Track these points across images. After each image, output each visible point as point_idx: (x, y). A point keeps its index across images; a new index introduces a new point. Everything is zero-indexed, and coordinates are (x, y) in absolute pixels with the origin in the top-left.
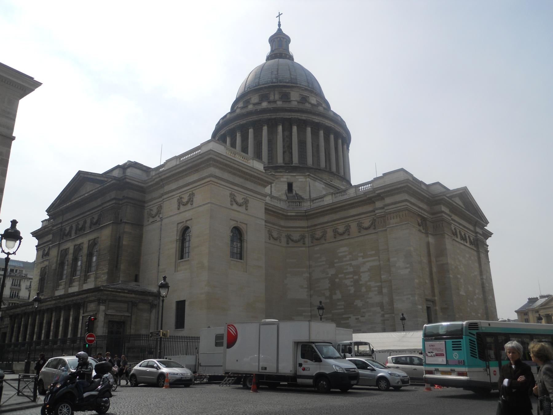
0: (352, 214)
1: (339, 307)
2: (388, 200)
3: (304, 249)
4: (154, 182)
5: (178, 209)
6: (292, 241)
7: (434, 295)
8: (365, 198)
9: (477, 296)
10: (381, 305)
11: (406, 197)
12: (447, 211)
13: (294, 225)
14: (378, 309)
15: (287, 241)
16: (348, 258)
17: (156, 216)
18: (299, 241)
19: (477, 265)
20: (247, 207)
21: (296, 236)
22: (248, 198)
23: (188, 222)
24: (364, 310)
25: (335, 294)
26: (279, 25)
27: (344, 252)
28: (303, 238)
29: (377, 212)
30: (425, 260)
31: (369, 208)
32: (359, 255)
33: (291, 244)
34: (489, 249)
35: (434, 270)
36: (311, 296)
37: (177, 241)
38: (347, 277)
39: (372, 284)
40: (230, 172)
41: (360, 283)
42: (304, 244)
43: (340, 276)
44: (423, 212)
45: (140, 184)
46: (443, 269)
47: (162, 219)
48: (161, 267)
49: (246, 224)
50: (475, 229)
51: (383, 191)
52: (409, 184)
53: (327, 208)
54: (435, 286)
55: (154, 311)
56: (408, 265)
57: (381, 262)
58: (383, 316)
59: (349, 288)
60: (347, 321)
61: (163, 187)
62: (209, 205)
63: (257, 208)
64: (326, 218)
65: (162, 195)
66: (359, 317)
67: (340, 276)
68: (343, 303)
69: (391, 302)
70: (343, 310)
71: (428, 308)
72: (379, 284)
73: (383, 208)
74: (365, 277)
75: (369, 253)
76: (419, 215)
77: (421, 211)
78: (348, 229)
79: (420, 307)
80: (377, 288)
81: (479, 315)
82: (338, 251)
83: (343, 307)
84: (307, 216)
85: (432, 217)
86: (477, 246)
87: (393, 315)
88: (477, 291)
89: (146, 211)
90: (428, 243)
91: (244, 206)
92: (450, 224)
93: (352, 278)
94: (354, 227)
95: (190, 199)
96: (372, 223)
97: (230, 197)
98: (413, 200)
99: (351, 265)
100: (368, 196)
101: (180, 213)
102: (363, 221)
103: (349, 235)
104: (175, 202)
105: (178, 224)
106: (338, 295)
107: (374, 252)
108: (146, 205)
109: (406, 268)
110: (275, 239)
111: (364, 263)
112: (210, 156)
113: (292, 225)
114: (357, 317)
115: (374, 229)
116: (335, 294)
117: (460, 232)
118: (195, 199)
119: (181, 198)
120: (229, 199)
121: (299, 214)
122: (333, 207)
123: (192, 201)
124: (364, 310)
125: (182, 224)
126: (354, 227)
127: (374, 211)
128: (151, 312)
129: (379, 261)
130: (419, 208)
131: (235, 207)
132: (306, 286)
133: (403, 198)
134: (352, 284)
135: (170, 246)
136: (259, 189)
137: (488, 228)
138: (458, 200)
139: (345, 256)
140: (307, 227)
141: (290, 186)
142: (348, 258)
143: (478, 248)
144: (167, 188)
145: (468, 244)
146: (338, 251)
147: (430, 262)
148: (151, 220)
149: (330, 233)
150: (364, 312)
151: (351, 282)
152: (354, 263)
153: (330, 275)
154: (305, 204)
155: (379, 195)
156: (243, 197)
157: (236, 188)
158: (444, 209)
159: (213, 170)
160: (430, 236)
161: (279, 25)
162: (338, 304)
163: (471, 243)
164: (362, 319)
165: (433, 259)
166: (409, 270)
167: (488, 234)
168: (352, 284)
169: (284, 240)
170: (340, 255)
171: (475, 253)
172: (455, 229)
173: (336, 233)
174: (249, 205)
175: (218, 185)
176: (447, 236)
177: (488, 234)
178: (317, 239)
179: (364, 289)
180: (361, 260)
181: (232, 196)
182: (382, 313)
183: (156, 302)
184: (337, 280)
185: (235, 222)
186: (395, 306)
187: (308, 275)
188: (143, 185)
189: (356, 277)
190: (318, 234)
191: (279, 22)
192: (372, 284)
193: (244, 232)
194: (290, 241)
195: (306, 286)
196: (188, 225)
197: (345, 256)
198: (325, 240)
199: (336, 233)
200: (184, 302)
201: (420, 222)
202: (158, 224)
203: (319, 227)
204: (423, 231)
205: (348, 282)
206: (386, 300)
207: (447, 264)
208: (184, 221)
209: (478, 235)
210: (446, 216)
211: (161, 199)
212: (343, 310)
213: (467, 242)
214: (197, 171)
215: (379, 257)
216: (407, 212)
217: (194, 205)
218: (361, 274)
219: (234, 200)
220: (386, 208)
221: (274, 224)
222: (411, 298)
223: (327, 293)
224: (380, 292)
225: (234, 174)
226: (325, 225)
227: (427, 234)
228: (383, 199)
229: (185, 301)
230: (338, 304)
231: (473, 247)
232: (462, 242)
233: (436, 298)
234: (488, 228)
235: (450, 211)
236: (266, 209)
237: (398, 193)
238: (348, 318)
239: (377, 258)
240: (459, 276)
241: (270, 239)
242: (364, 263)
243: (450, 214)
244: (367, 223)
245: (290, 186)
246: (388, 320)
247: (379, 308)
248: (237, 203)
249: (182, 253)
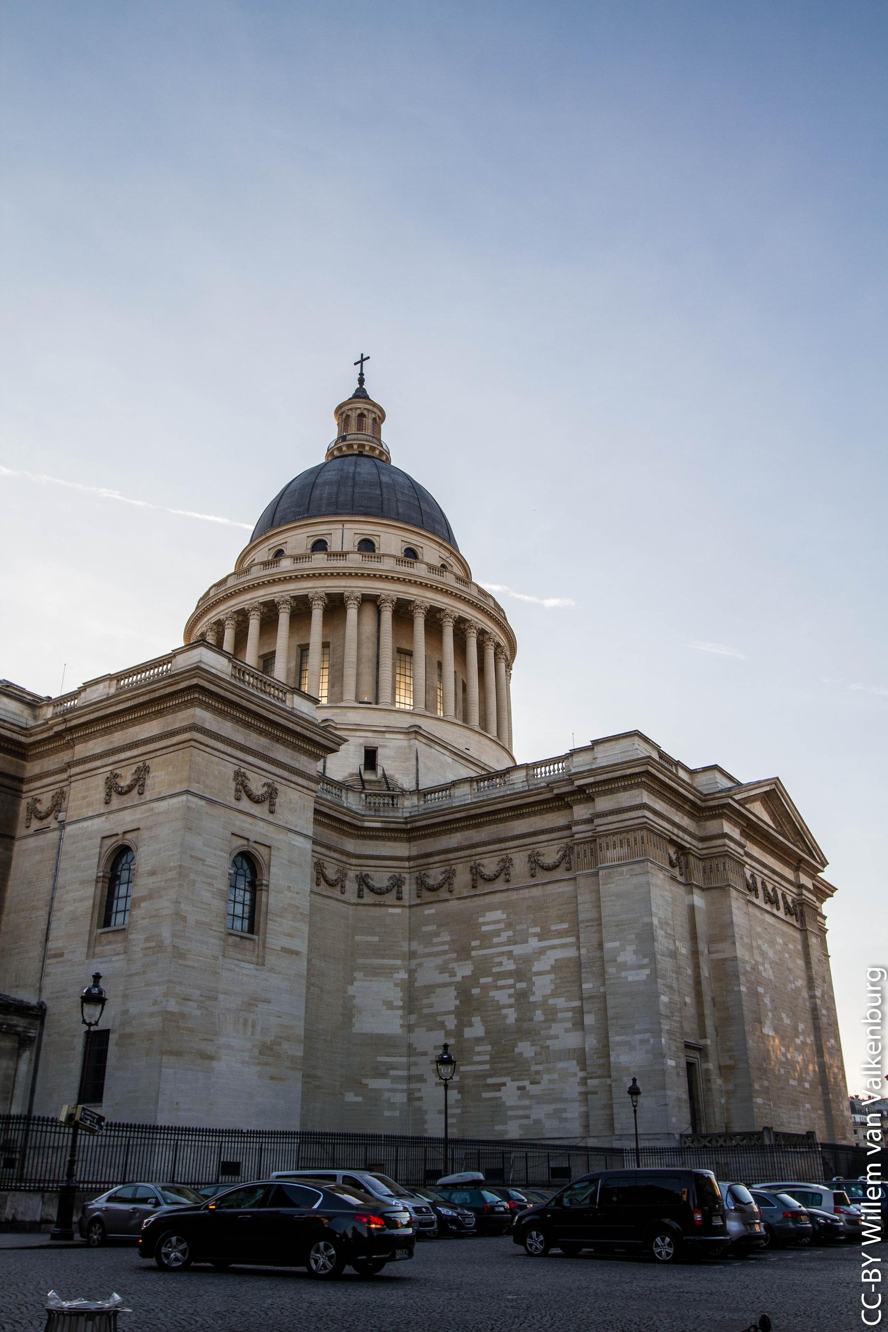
0: (516, 832)
1: (477, 1058)
2: (603, 804)
3: (398, 910)
4: (51, 733)
5: (107, 803)
6: (372, 890)
7: (704, 1036)
8: (549, 795)
9: (801, 1038)
10: (581, 1057)
11: (646, 797)
12: (736, 833)
13: (377, 853)
14: (572, 1066)
15: (360, 890)
16: (504, 937)
17: (47, 815)
18: (388, 890)
19: (800, 962)
20: (272, 804)
21: (380, 879)
22: (277, 785)
23: (128, 836)
24: (539, 1068)
25: (471, 1025)
26: (361, 381)
27: (494, 922)
28: (397, 883)
29: (575, 829)
30: (684, 950)
31: (557, 819)
32: (531, 930)
33: (369, 897)
34: (828, 924)
35: (705, 972)
36: (410, 1028)
37: (97, 882)
38: (500, 983)
39: (560, 1002)
40: (238, 721)
41: (532, 999)
42: (399, 898)
43: (483, 980)
44: (681, 834)
45: (15, 736)
46: (727, 971)
47: (62, 825)
48: (51, 945)
49: (269, 847)
50: (797, 877)
51: (591, 780)
52: (650, 769)
53: (458, 815)
54: (707, 1012)
55: (26, 1055)
56: (646, 961)
57: (583, 951)
58: (584, 1081)
59: (504, 1011)
60: (498, 1094)
61: (70, 745)
62: (184, 798)
63: (297, 807)
64: (455, 839)
65: (69, 765)
66: (526, 1083)
67: (483, 980)
68: (489, 1048)
69: (605, 1049)
70: (487, 1067)
71: (690, 1066)
72: (576, 1003)
73: (590, 821)
74: (543, 986)
75: (553, 928)
76: (672, 842)
77: (676, 831)
78: (505, 866)
79: (671, 1063)
80: (570, 1014)
81: (807, 1085)
82: (481, 920)
83: (487, 1058)
84: (410, 831)
85: (700, 845)
86: (801, 918)
87: (608, 1081)
88: (801, 1027)
89: (24, 803)
90: (692, 908)
91: (267, 803)
92: (742, 864)
93: (510, 987)
94: (520, 862)
95: (137, 780)
96: (564, 856)
97: (235, 779)
98: (660, 805)
99: (510, 954)
100: (556, 791)
101: (110, 813)
102: (542, 850)
103: (508, 881)
104: (97, 786)
105: (103, 838)
106: (476, 1029)
107: (565, 926)
108: (25, 788)
109: (641, 967)
110: (331, 884)
111: (542, 951)
112: (195, 681)
113: (371, 853)
114: (521, 1083)
115: (568, 870)
116: (471, 1025)
117: (763, 883)
118: (149, 782)
119: (116, 776)
120: (232, 785)
121: (393, 826)
122: (473, 812)
123: (143, 785)
124: (539, 1068)
125: (114, 839)
126: (520, 862)
127: (568, 827)
128: (19, 1056)
129: (578, 948)
130: (674, 824)
131: (245, 804)
132: (401, 1004)
133: (637, 801)
134: (512, 1001)
135: (79, 895)
136: (303, 762)
137: (826, 875)
138: (758, 810)
139: (497, 933)
140: (409, 859)
142: (504, 937)
143: (803, 923)
144: (82, 750)
145: (781, 914)
146: (481, 920)
147: (695, 953)
148: (36, 824)
149: (463, 876)
150: (537, 1073)
151: (510, 996)
152: (518, 950)
153: (458, 978)
154: (407, 803)
155: (581, 789)
156: (265, 780)
157: (250, 759)
158: (728, 828)
159: (201, 715)
160: (695, 890)
161: (361, 381)
162: (477, 1049)
164: (533, 1089)
165: (702, 947)
166: (647, 971)
167: (825, 891)
168: (512, 1001)
169: (351, 886)
170: (484, 928)
171: (797, 935)
172: (752, 876)
173: (478, 877)
174: (277, 800)
175: (208, 750)
176: (734, 893)
177: (825, 891)
178: (432, 889)
179: (539, 1016)
180: (534, 943)
181: (240, 778)
182: (581, 1074)
183: (33, 1033)
184: (475, 991)
185: (245, 842)
186: (612, 1059)
187: (406, 976)
188: (23, 739)
189: (522, 985)
190: (435, 875)
191: (361, 374)
192: (560, 1002)
193: (263, 866)
194: (366, 890)
195: (401, 1004)
196: (126, 842)
197: (497, 933)
198: (451, 891)
199: (478, 877)
200: (104, 1035)
201: (674, 857)
202: (53, 836)
203: (437, 858)
204: (679, 878)
205: (502, 997)
206: (591, 1042)
207: (735, 958)
208: (120, 832)
209: (805, 892)
210: (732, 845)
211: (64, 776)
212: (487, 1067)
213: (778, 909)
214: (160, 713)
215: (578, 938)
216: (645, 833)
217: (148, 796)
218: (534, 978)
219: (245, 787)
220: (597, 821)
221: (329, 848)
222: (651, 1040)
223: (451, 1023)
224: (579, 1024)
225: (248, 726)
226: (451, 856)
227: (689, 886)
228: (590, 799)
229: (107, 1032)
230: (477, 1049)
231: (792, 920)
232: (767, 907)
233: (709, 1042)
234: (826, 875)
235: (743, 833)
236: (316, 811)
237: (625, 789)
238: (498, 1087)
239: (572, 939)
240: (761, 990)
241: (318, 885)
242: (542, 951)
243: (743, 841)
244: (551, 855)
246: (596, 1093)
247: (575, 1062)
248: (250, 796)
249: (106, 913)
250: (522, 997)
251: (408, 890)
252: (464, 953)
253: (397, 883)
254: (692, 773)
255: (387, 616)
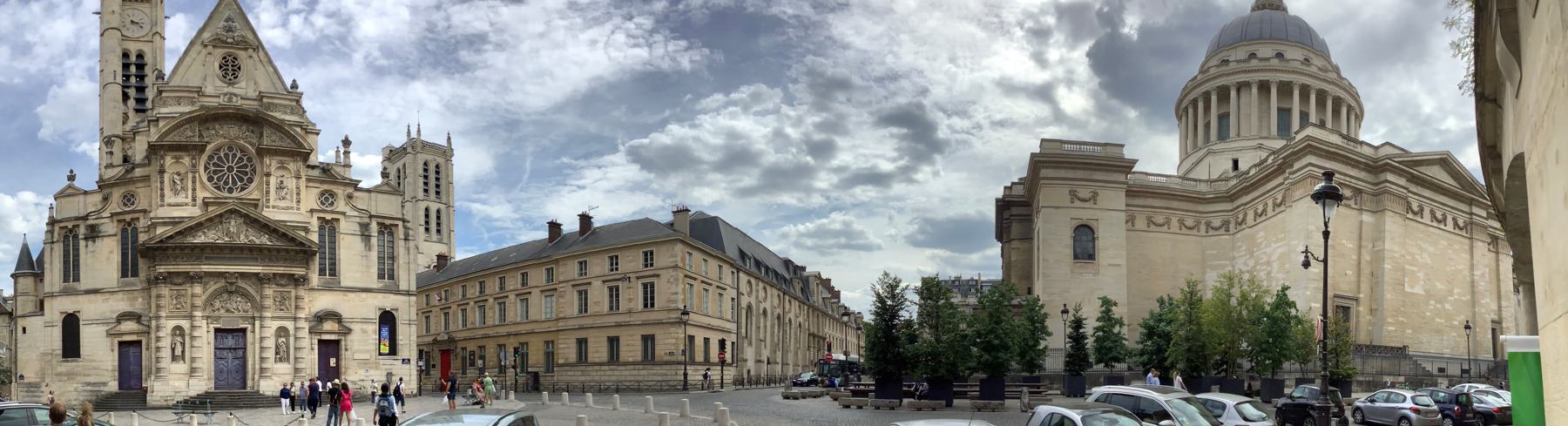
21: (1217, 222)
28: (1226, 224)
35: (1366, 257)
141: (1236, 163)
163: (1456, 224)
169: (1203, 227)
205: (1262, 275)
245: (1236, 163)
250: (1269, 273)
251: (1232, 226)
252: (1252, 254)
253: (1226, 224)
254: (1376, 148)
255: (1255, 90)
